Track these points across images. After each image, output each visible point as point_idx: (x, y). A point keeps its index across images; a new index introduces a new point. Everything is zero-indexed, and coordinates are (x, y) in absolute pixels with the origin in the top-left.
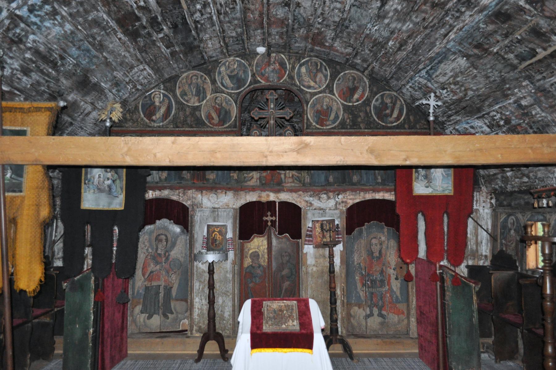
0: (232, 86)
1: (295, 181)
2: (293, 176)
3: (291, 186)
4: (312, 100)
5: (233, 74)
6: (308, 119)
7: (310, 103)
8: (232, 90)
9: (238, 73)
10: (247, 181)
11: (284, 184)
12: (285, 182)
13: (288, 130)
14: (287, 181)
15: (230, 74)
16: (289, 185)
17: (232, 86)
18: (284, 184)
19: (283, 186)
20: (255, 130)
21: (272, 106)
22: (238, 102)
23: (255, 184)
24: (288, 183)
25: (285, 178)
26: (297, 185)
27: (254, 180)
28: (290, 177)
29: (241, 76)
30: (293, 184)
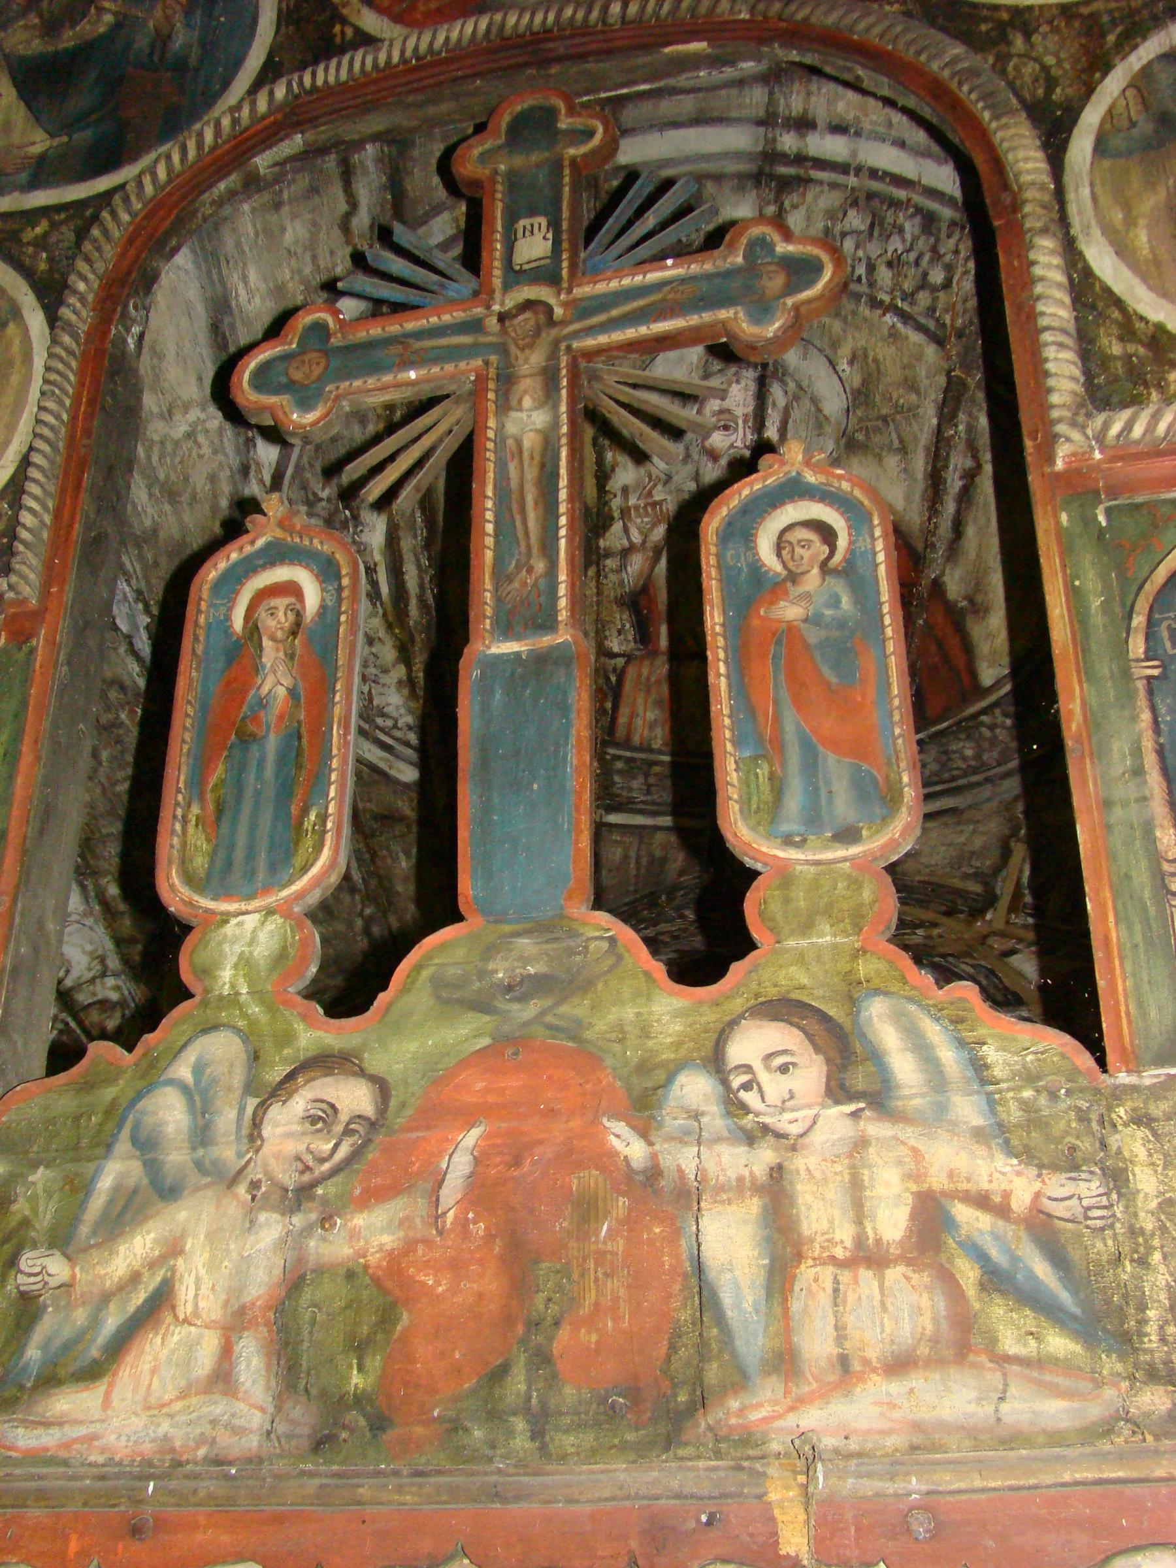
0: (39, 142)
1: (1012, 1331)
2: (931, 1219)
3: (924, 1445)
4: (1113, 85)
5: (68, 39)
6: (1084, 288)
7: (1091, 117)
8: (34, 184)
9: (118, 26)
10: (50, 1380)
11: (761, 1406)
12: (785, 1361)
13: (794, 490)
14: (817, 1344)
15: (37, 46)
16: (864, 1413)
17: (39, 142)
18: (761, 1406)
19: (747, 1442)
20: (276, 555)
21: (534, 246)
22: (85, 283)
23: (182, 1428)
24: (846, 1371)
25: (780, 1276)
26: (1055, 1411)
27: (165, 1361)
28: (868, 1256)
29: (162, 39)
30: (953, 1399)
